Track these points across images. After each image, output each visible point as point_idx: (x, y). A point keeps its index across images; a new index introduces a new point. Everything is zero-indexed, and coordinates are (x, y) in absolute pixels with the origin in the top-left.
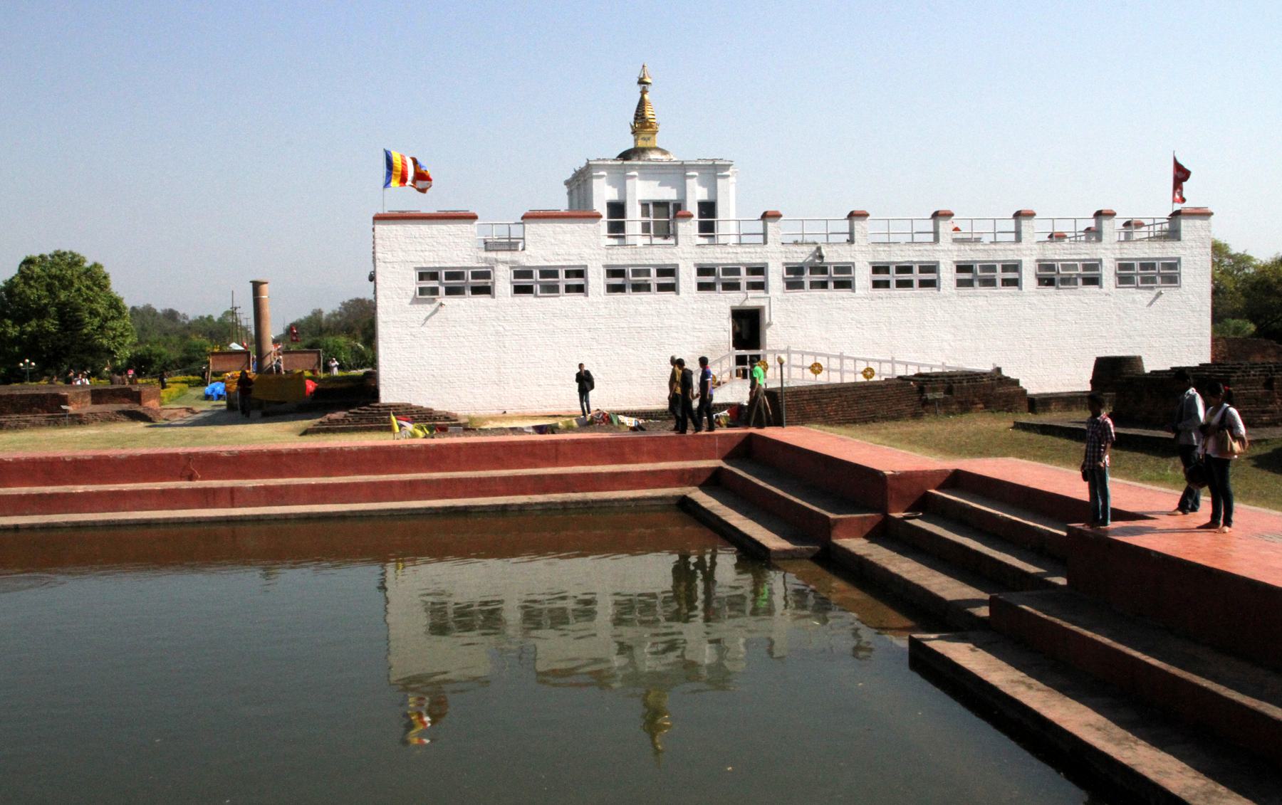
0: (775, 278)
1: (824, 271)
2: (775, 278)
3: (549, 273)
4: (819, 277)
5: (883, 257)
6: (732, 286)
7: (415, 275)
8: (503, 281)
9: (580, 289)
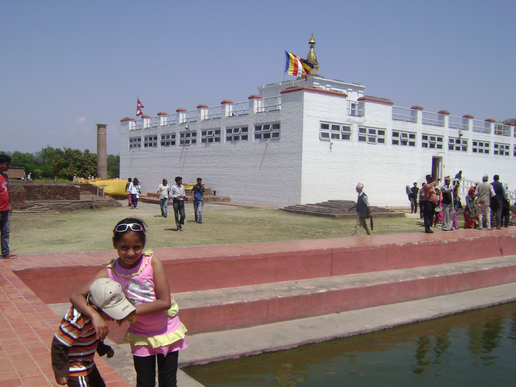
0: (445, 143)
1: (458, 142)
2: (445, 143)
3: (372, 131)
4: (458, 145)
5: (476, 138)
6: (432, 146)
7: (319, 125)
8: (355, 134)
9: (381, 141)
